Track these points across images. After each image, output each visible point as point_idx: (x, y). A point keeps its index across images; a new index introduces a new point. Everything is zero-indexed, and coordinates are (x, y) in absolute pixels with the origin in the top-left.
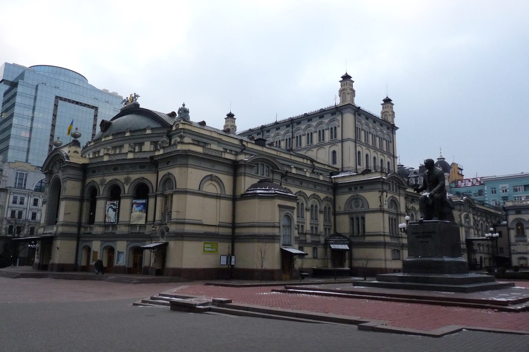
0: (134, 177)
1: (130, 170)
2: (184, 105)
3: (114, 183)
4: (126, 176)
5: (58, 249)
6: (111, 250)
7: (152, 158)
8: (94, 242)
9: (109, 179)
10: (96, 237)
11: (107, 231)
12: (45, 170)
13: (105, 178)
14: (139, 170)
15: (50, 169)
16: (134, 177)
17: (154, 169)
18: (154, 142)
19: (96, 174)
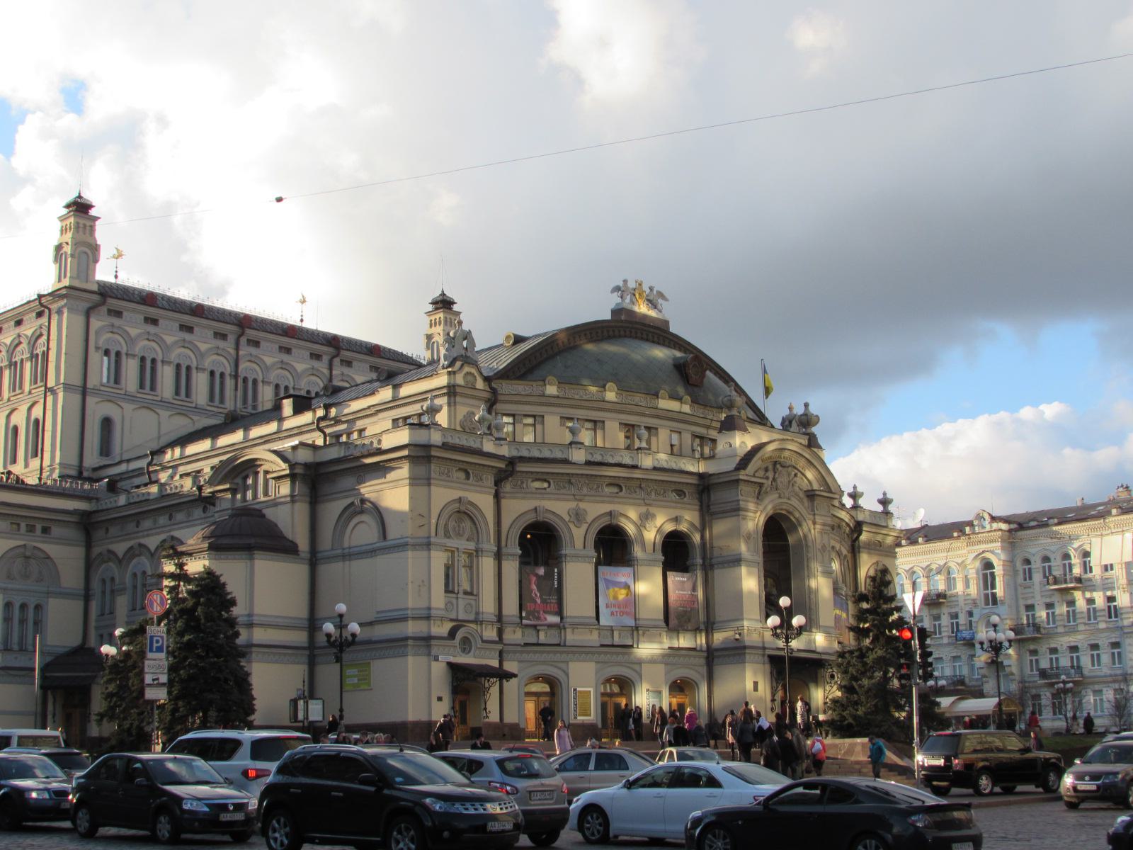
2: (790, 408)
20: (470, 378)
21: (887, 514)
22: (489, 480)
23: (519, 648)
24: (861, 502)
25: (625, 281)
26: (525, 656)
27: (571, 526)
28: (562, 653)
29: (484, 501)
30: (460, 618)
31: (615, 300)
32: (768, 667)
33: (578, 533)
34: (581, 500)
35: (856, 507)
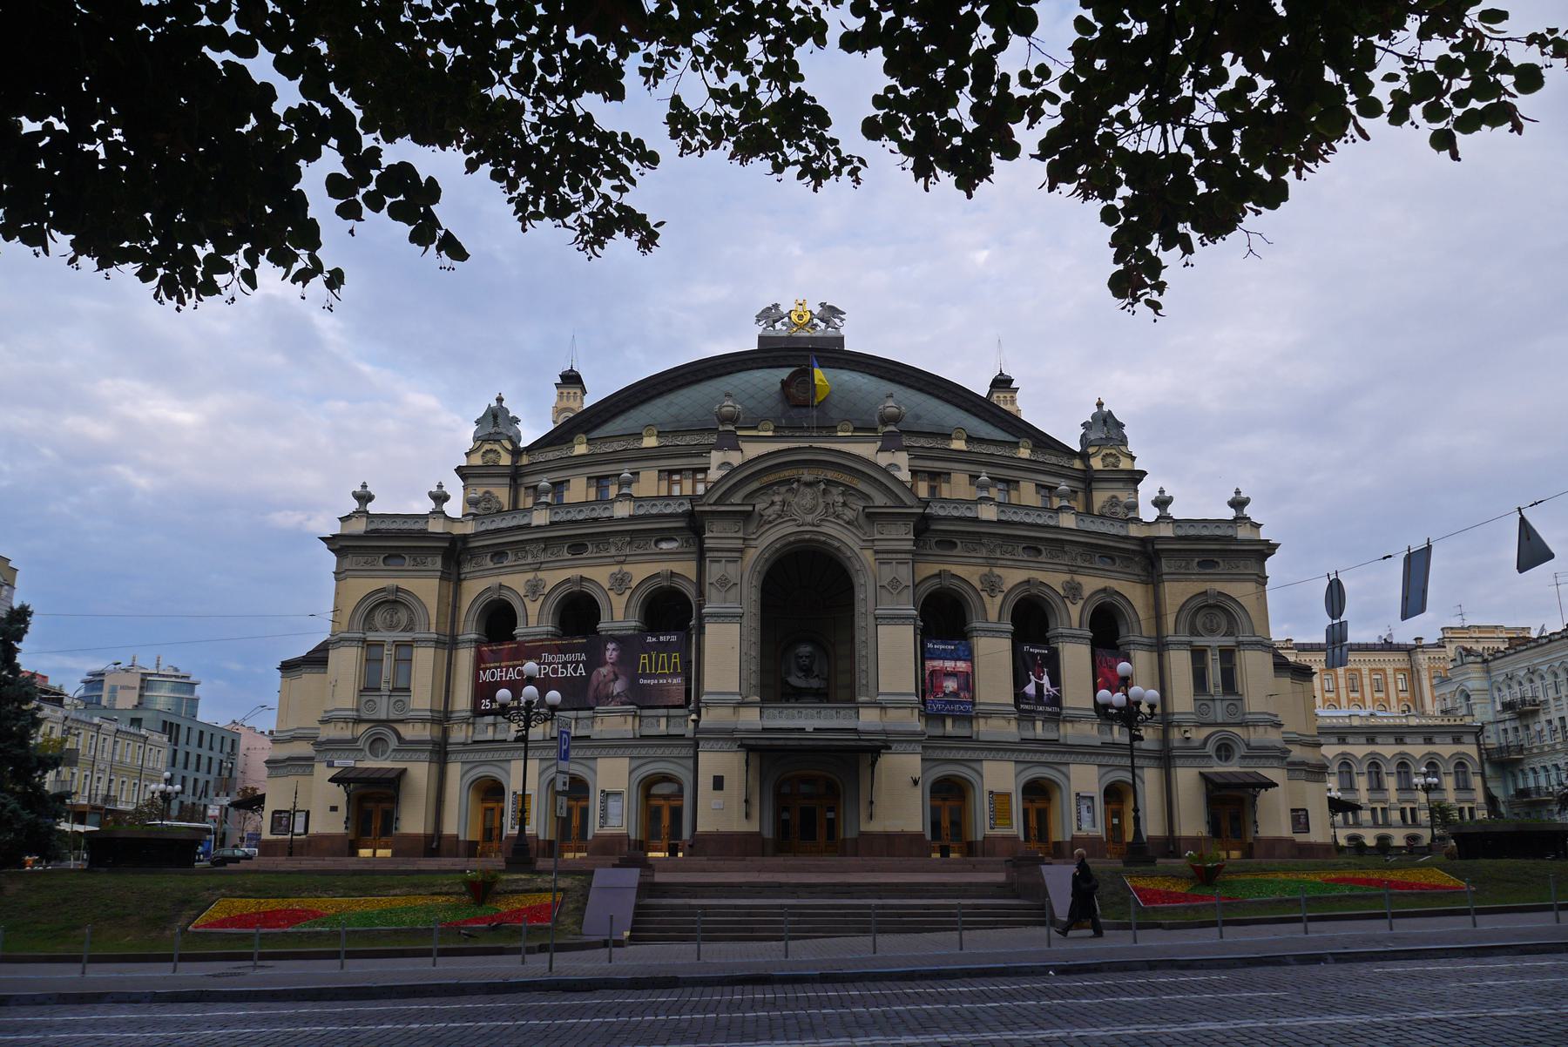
0: (1091, 584)
1: (1079, 562)
2: (1100, 405)
3: (1034, 591)
4: (1067, 577)
5: (916, 782)
6: (1038, 792)
7: (1144, 541)
8: (985, 764)
9: (1012, 577)
10: (998, 748)
11: (1029, 735)
12: (714, 504)
13: (997, 571)
14: (1101, 566)
15: (737, 499)
16: (1091, 584)
17: (1137, 570)
18: (1044, 487)
19: (954, 553)
20: (491, 455)
21: (1240, 520)
22: (438, 563)
23: (461, 748)
24: (1174, 511)
25: (776, 306)
26: (471, 757)
27: (526, 600)
28: (503, 750)
29: (425, 588)
30: (383, 716)
31: (759, 330)
32: (742, 756)
33: (533, 608)
34: (538, 569)
35: (1164, 518)
